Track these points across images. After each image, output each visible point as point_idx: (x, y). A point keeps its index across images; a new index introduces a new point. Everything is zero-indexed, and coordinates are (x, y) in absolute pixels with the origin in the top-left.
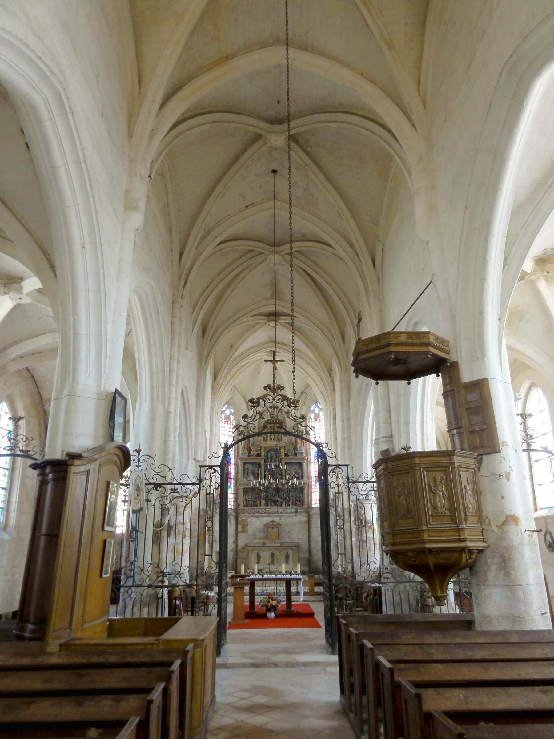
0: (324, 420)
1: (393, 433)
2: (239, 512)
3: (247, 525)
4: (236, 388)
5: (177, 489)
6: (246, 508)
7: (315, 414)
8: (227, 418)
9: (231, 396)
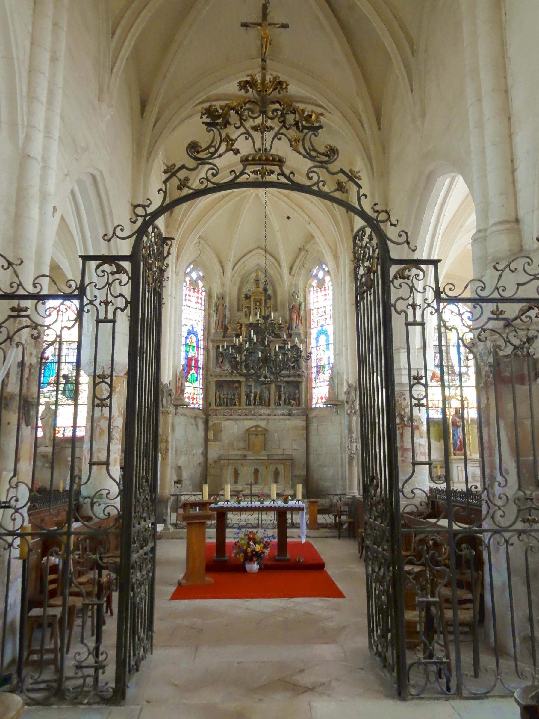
0: (331, 288)
1: (521, 213)
2: (210, 413)
3: (221, 431)
4: (206, 241)
5: (26, 309)
6: (220, 408)
7: (319, 280)
8: (194, 284)
9: (199, 252)
